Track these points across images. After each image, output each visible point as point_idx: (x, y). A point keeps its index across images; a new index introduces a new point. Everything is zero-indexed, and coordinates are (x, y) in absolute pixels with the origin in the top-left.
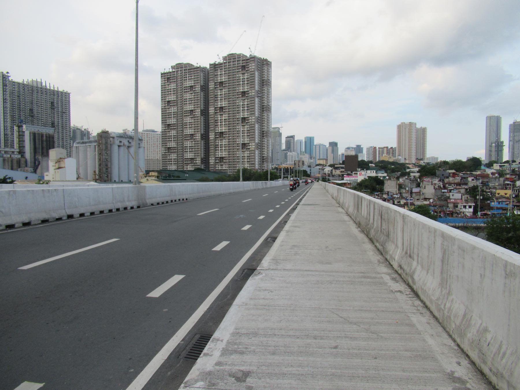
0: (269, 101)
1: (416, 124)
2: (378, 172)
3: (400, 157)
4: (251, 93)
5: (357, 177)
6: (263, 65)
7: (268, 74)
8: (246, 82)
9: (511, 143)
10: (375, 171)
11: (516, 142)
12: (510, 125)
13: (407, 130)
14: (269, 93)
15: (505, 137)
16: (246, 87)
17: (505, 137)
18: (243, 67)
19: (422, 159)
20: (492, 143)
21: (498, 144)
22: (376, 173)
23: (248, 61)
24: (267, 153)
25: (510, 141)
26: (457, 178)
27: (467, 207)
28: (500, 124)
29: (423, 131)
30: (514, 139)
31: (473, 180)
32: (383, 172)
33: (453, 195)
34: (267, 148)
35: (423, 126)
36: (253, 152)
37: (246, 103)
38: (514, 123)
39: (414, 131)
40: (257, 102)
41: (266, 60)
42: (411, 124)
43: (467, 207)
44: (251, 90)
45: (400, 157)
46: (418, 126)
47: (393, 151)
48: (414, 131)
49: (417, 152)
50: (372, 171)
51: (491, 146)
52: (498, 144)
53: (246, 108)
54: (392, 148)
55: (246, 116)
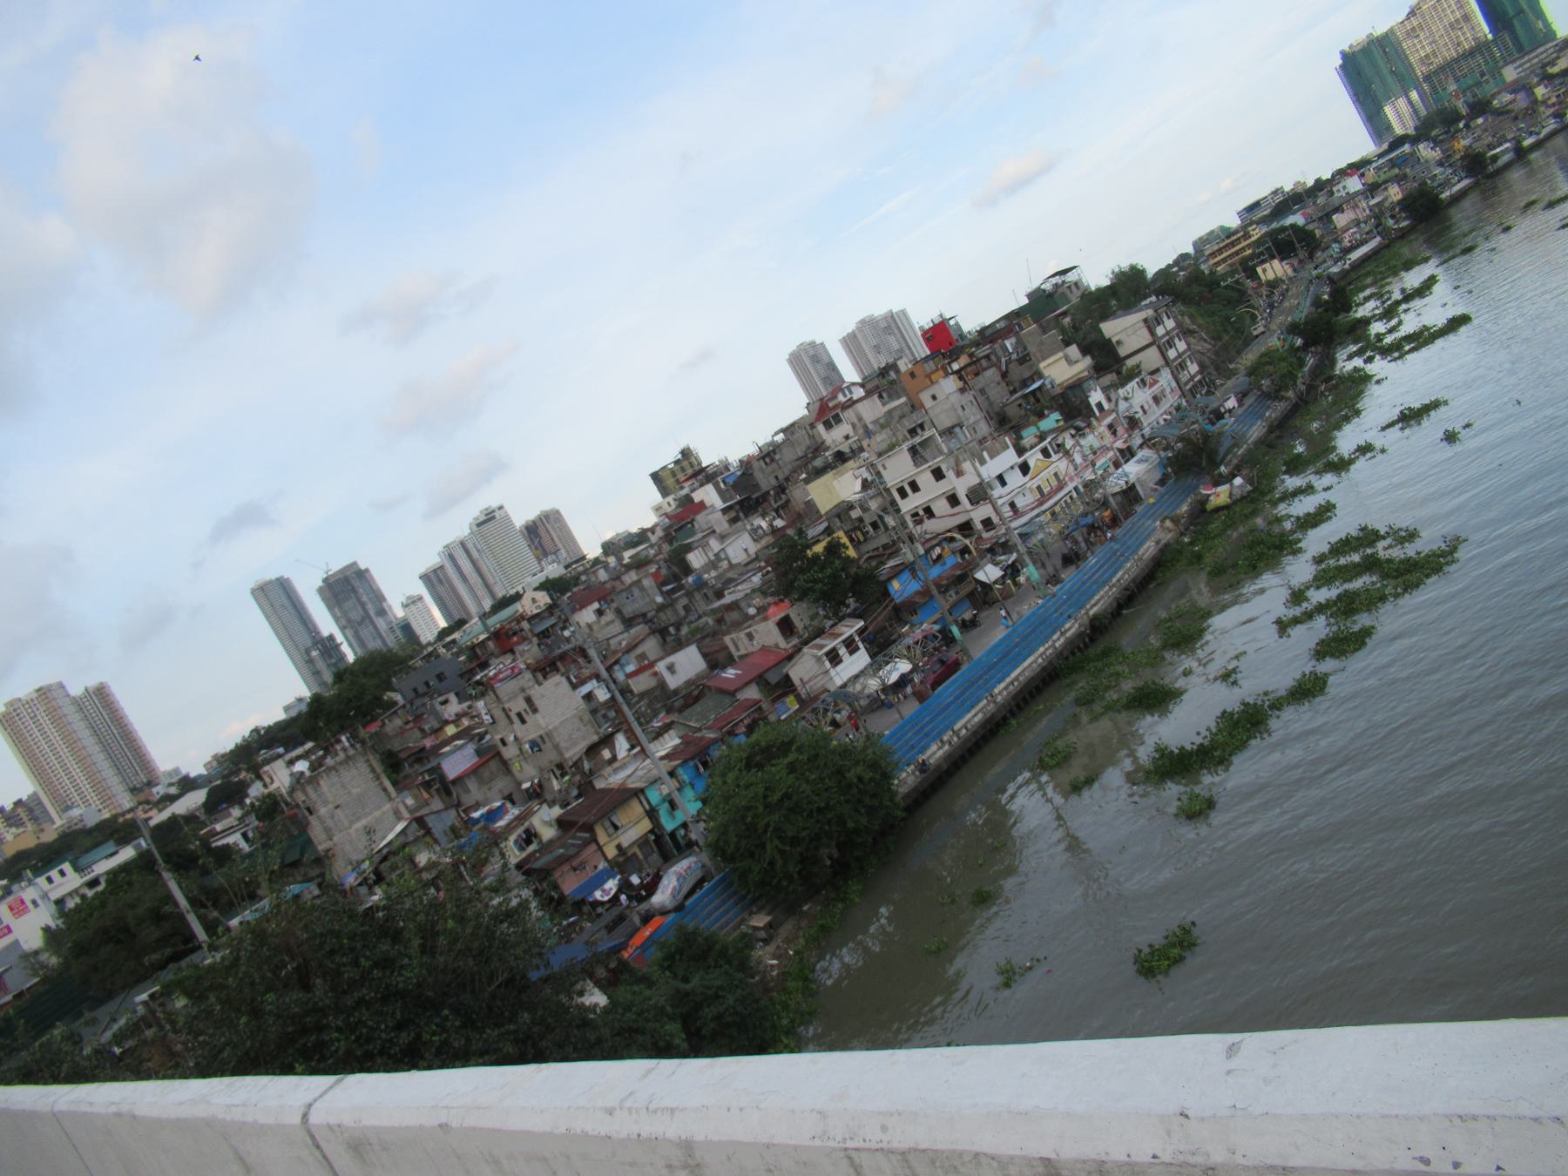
1: (61, 686)
2: (83, 861)
3: (75, 812)
5: (9, 930)
9: (349, 632)
10: (67, 867)
11: (360, 624)
12: (321, 591)
13: (42, 716)
15: (326, 624)
17: (326, 624)
19: (151, 784)
20: (308, 652)
21: (324, 646)
22: (77, 869)
25: (343, 629)
26: (524, 647)
27: (842, 651)
28: (295, 592)
29: (101, 695)
30: (349, 621)
31: (600, 612)
32: (110, 847)
33: (671, 668)
35: (93, 682)
38: (325, 580)
39: (69, 710)
42: (43, 693)
43: (842, 651)
45: (75, 812)
46: (76, 690)
47: (31, 811)
48: (69, 710)
49: (119, 771)
50: (54, 874)
51: (310, 661)
52: (324, 646)
54: (19, 803)
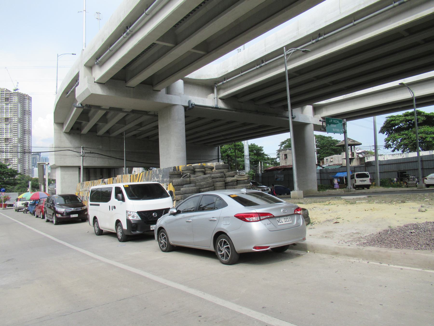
0: (30, 126)
4: (15, 120)
6: (24, 99)
7: (28, 106)
8: (9, 111)
14: (30, 121)
16: (9, 115)
18: (7, 99)
23: (11, 95)
24: (28, 166)
34: (28, 162)
36: (16, 165)
37: (9, 127)
40: (19, 127)
41: (27, 95)
44: (15, 117)
53: (9, 131)
55: (9, 137)
